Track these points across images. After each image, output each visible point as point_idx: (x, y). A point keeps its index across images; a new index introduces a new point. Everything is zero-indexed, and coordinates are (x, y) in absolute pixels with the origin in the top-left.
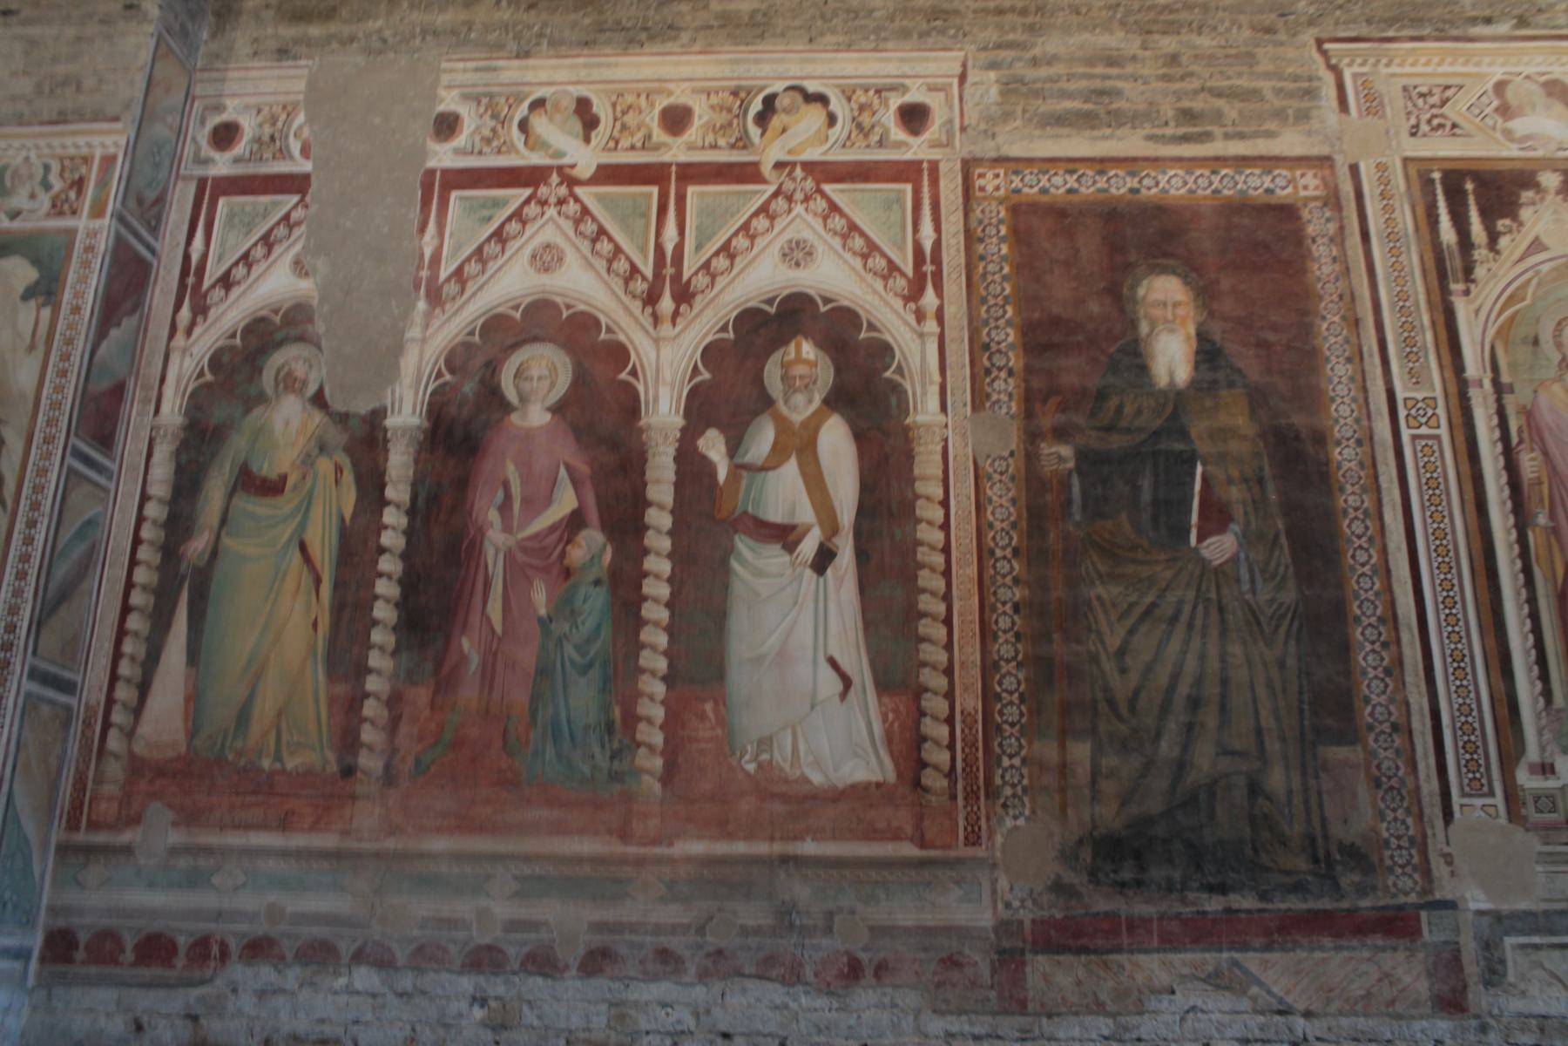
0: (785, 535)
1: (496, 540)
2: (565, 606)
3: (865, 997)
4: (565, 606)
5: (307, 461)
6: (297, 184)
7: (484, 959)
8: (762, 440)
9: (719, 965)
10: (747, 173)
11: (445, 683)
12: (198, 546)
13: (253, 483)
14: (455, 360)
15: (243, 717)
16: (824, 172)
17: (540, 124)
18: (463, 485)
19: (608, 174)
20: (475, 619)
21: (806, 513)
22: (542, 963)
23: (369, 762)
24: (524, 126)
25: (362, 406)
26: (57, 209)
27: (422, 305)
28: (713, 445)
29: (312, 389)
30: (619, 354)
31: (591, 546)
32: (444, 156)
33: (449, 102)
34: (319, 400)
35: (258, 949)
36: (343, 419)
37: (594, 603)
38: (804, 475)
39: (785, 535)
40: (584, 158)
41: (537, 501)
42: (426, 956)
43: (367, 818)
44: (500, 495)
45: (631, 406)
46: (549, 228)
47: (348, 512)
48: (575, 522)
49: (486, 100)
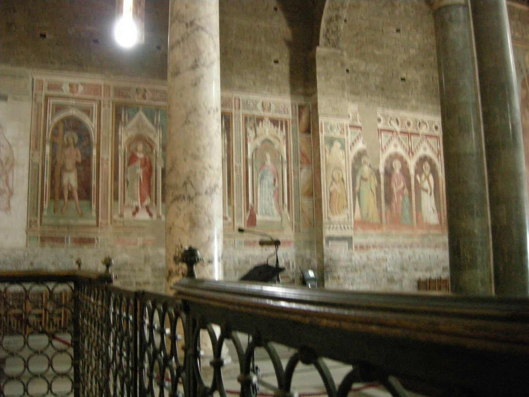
0: (426, 191)
1: (395, 190)
2: (404, 199)
3: (437, 250)
4: (404, 199)
5: (370, 177)
6: (360, 128)
7: (399, 246)
8: (423, 177)
9: (423, 246)
10: (417, 135)
11: (391, 210)
12: (357, 188)
13: (362, 178)
14: (387, 161)
15: (368, 215)
16: (427, 136)
17: (392, 122)
18: (390, 182)
19: (402, 132)
20: (394, 201)
21: (428, 187)
22: (406, 247)
23: (384, 221)
24: (390, 122)
25: (376, 167)
26: (341, 133)
27: (381, 151)
28: (418, 178)
29: (369, 164)
30: (406, 163)
31: (406, 191)
32: (380, 126)
33: (379, 115)
34: (370, 166)
35: (374, 246)
36: (374, 170)
37: (407, 199)
38: (428, 182)
39: (426, 191)
40: (398, 129)
41: (399, 183)
42: (393, 246)
43: (385, 229)
44: (394, 182)
45: (408, 171)
46: (395, 141)
47: (376, 185)
48: (404, 188)
49: (386, 117)
